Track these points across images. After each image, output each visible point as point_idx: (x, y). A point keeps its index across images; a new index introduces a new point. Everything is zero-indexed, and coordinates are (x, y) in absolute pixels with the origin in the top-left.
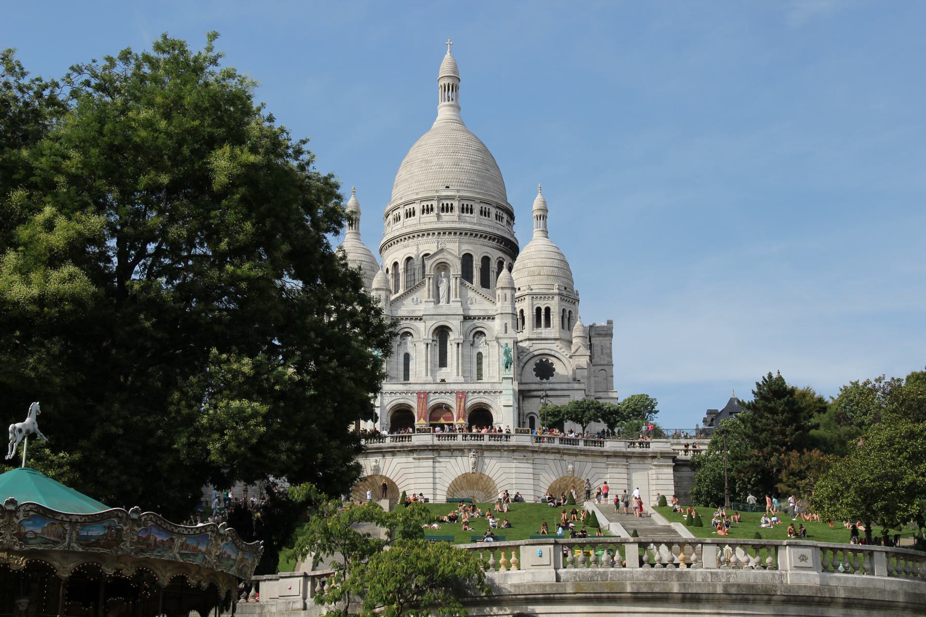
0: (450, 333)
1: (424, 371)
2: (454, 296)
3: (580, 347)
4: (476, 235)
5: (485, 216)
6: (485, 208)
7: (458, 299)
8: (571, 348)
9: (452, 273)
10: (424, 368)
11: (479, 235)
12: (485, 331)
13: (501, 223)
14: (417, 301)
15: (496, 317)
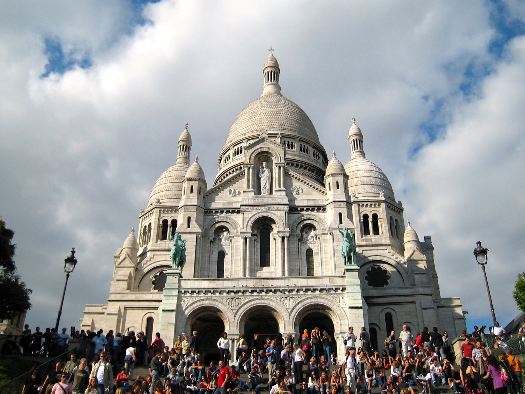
0: (273, 226)
1: (242, 270)
2: (277, 185)
3: (415, 251)
4: (297, 165)
5: (304, 152)
6: (304, 146)
7: (282, 188)
8: (403, 256)
9: (274, 161)
10: (242, 267)
11: (300, 165)
12: (315, 224)
13: (318, 160)
14: (235, 192)
15: (327, 207)
